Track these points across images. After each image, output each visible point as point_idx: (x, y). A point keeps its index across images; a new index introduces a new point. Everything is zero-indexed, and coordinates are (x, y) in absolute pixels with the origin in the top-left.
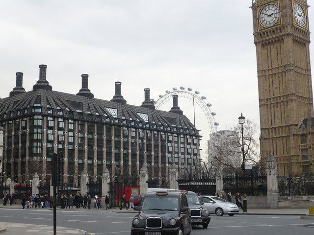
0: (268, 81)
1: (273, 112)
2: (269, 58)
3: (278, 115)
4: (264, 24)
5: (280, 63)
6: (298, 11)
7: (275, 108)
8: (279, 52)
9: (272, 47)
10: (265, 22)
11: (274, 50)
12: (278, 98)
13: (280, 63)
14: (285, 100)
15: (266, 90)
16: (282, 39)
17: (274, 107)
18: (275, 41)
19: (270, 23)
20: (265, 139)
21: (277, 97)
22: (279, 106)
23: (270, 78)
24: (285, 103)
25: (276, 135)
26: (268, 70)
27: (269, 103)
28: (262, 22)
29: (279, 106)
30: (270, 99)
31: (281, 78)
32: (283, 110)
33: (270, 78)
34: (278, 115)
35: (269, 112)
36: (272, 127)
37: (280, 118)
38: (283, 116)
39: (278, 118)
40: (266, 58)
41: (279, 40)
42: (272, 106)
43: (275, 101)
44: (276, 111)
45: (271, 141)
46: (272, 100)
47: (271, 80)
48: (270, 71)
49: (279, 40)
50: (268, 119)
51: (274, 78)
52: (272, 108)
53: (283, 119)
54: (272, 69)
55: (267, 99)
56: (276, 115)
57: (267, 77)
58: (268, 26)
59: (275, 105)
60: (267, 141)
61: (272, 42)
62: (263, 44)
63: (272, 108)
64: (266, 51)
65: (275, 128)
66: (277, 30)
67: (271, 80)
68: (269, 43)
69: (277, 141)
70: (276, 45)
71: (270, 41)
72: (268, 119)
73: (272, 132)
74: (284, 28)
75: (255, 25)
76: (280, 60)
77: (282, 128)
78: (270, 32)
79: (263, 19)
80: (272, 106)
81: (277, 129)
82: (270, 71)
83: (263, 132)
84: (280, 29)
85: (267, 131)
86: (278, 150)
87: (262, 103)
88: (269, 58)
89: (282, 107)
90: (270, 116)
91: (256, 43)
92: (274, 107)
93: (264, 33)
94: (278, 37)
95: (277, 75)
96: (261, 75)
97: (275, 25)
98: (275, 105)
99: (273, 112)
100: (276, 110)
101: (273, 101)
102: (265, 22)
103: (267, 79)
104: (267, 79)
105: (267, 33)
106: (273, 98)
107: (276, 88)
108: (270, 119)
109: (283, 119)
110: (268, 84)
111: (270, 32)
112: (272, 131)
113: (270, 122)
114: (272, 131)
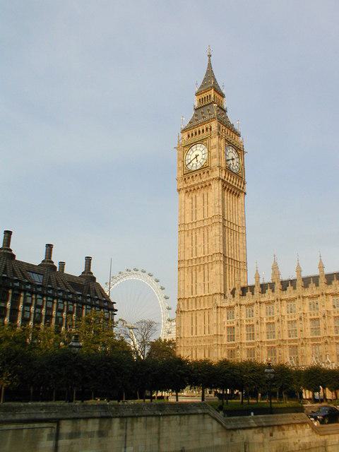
1: (194, 277)
3: (200, 280)
8: (206, 200)
9: (197, 195)
11: (199, 199)
16: (210, 185)
21: (200, 258)
26: (192, 224)
31: (206, 234)
32: (206, 275)
34: (200, 280)
46: (194, 261)
52: (194, 273)
53: (206, 286)
59: (198, 268)
63: (194, 273)
67: (194, 236)
71: (196, 187)
73: (192, 303)
89: (206, 271)
99: (194, 277)
100: (199, 274)
107: (200, 246)
109: (206, 286)
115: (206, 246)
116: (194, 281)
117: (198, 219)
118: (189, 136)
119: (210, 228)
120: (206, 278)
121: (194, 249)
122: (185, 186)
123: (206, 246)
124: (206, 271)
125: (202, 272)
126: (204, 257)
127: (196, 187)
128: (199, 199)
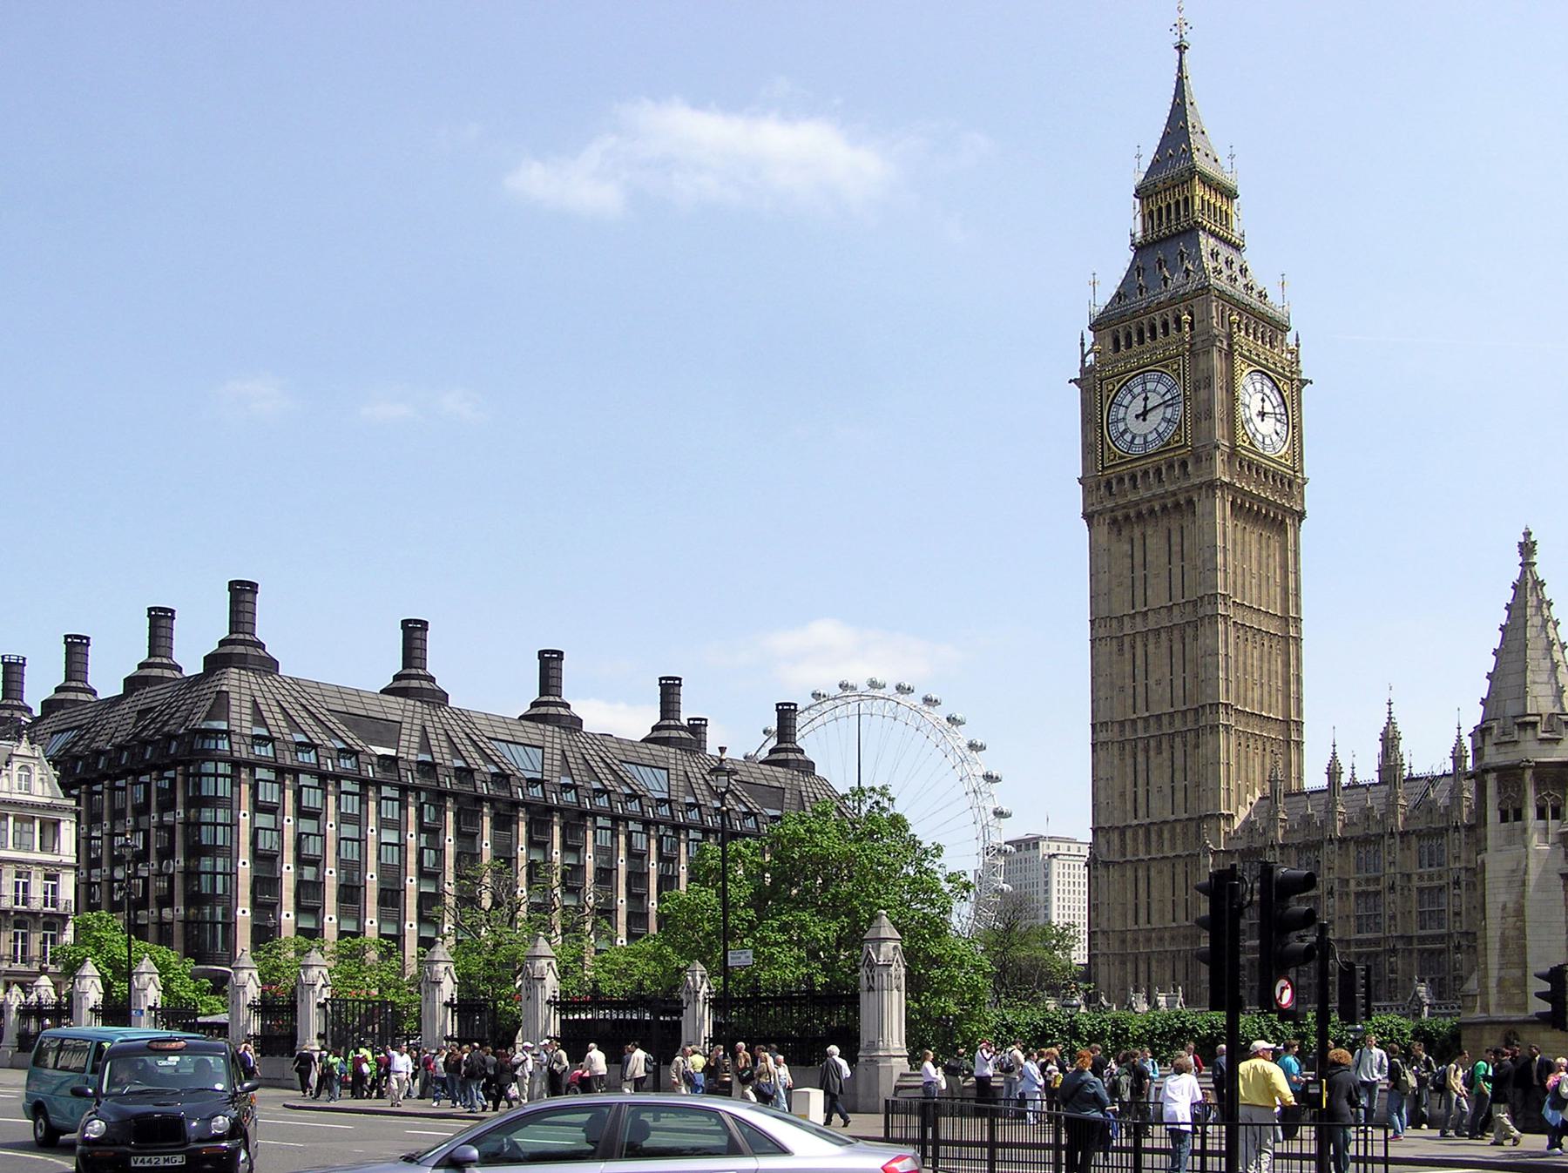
0: (1128, 655)
1: (1141, 767)
2: (1139, 573)
3: (1160, 778)
4: (1124, 447)
5: (1177, 591)
6: (1253, 395)
7: (1152, 753)
8: (1176, 548)
9: (1149, 532)
10: (1128, 437)
11: (1156, 542)
12: (1165, 720)
13: (1177, 591)
14: (1190, 725)
15: (1122, 689)
16: (1190, 502)
17: (1147, 750)
18: (1164, 508)
19: (1146, 442)
20: (1106, 864)
21: (1159, 717)
22: (1165, 746)
23: (1139, 644)
24: (1190, 737)
25: (1148, 852)
26: (1133, 617)
27: (1128, 735)
28: (1114, 435)
29: (1165, 746)
30: (1134, 722)
31: (1177, 647)
32: (1179, 762)
33: (1139, 644)
34: (1160, 778)
35: (1130, 770)
36: (1135, 822)
37: (1167, 790)
38: (1179, 784)
39: (1160, 789)
40: (1127, 573)
41: (1177, 505)
42: (1140, 745)
43: (1153, 731)
44: (1152, 765)
45: (1130, 873)
46: (1140, 724)
47: (1140, 651)
48: (1138, 619)
49: (1177, 505)
50: (1123, 794)
51: (1151, 647)
52: (1141, 758)
53: (1180, 796)
54: (1145, 614)
55: (1122, 724)
56: (1152, 780)
57: (1127, 640)
58: (1138, 451)
59: (1153, 743)
60: (1114, 873)
61: (1152, 511)
62: (1114, 521)
63: (1141, 758)
64: (1127, 547)
65: (1147, 828)
66: (1171, 466)
67: (1140, 651)
68: (1139, 515)
69: (1153, 873)
70: (1164, 522)
71: (1144, 508)
72: (1123, 794)
73: (1135, 840)
74: (1198, 460)
75: (1088, 449)
76: (1177, 581)
77: (1174, 829)
78: (1146, 473)
79: (1122, 427)
80: (1140, 745)
81: (1154, 829)
82: (1138, 619)
83: (1102, 840)
84: (1184, 464)
85: (1115, 837)
86: (1154, 907)
87: (1102, 736)
88: (1139, 573)
89: (1179, 754)
90: (1129, 787)
91: (1088, 516)
92: (1147, 750)
93: (1121, 480)
94: (1174, 494)
95: (1164, 635)
96: (1102, 632)
97: (1166, 447)
98: (1153, 743)
99: (1141, 767)
100: (1154, 761)
101: (1146, 729)
102: (1128, 437)
103: (1127, 646)
104: (1127, 646)
105: (1133, 478)
106: (1146, 719)
107: (1158, 683)
108: (1129, 796)
109: (1180, 796)
110: (1128, 669)
111: (1146, 473)
112: (1135, 834)
113: (1129, 806)
114: (1135, 834)
115: (1178, 683)
116: (1141, 781)
117: (1153, 603)
118: (1116, 342)
119: (1189, 631)
120: (1179, 775)
121: (1141, 690)
122: (1110, 504)
123: (1178, 683)
124: (1179, 754)
125: (1166, 754)
126: (1171, 715)
127: (1144, 508)
128: (1156, 542)
